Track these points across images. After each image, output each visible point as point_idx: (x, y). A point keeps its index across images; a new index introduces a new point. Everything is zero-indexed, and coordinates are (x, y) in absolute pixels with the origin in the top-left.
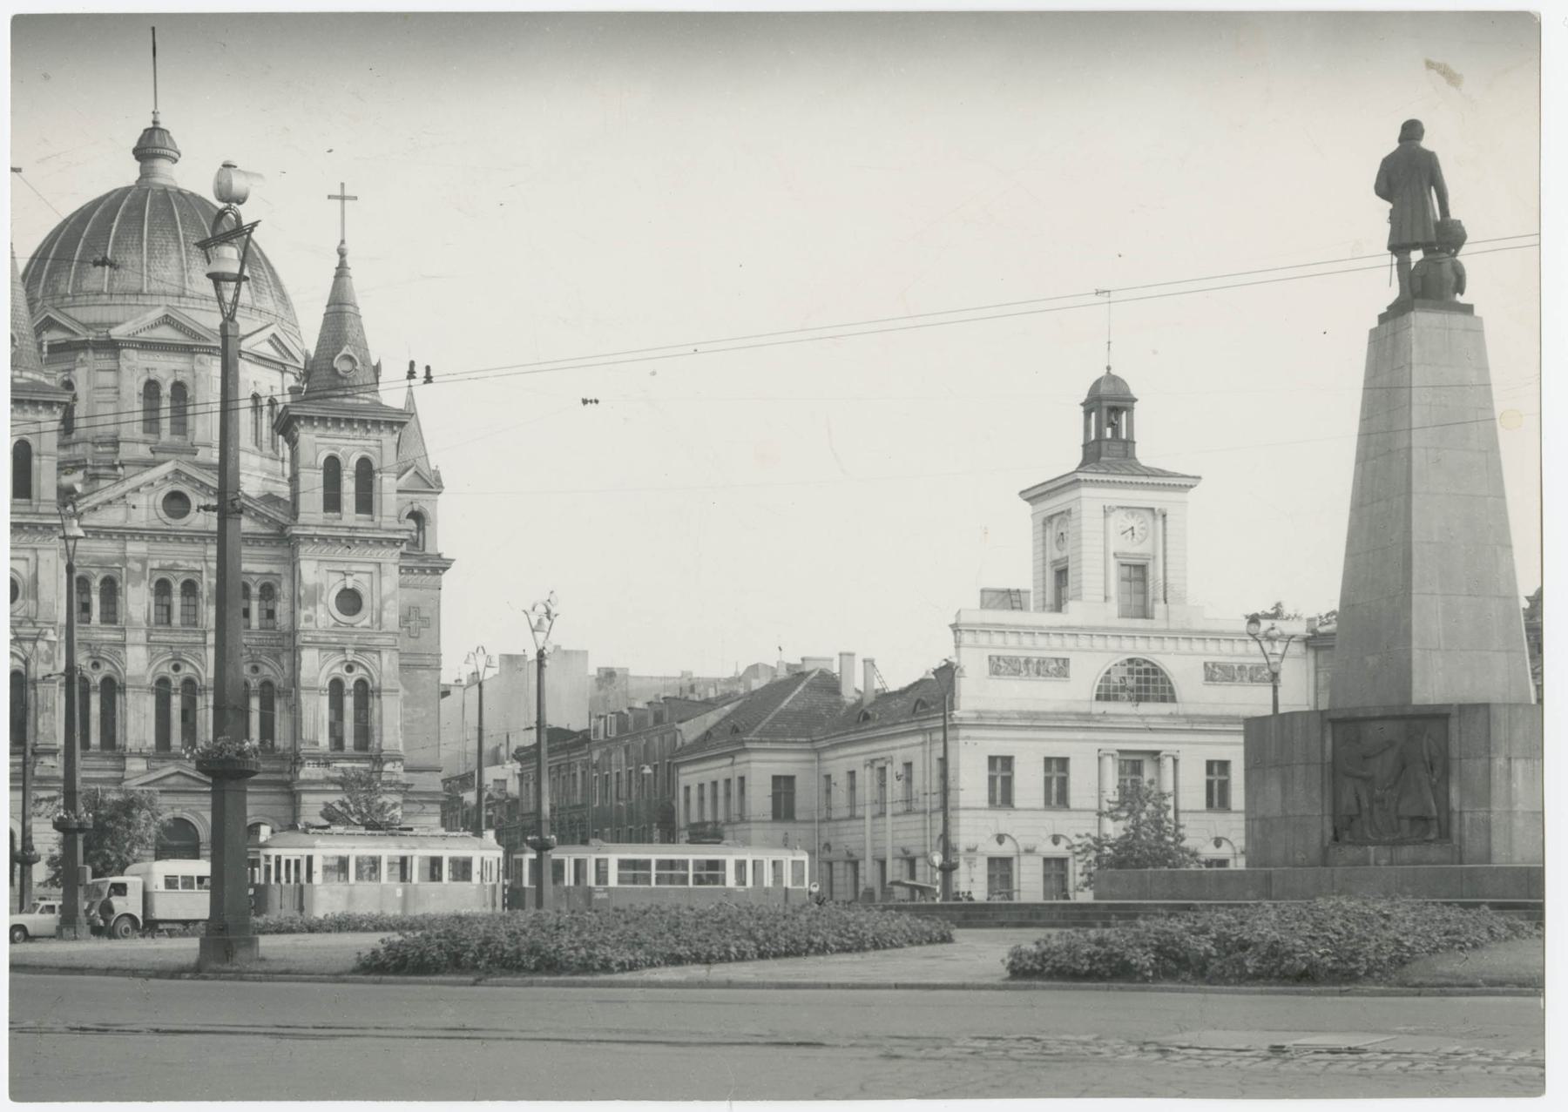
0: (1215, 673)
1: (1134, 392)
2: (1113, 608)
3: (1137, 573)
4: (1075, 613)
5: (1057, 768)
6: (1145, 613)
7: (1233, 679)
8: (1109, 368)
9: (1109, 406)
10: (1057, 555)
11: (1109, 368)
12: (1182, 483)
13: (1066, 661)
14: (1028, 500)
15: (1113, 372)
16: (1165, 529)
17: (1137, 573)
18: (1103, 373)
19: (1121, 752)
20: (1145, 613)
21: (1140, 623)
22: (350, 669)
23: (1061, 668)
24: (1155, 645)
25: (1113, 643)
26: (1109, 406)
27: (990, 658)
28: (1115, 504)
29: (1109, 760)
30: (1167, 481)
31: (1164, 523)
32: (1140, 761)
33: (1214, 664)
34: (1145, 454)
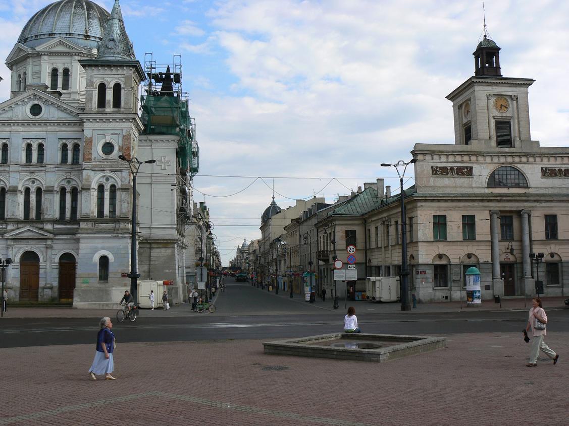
0: (547, 173)
1: (499, 45)
2: (494, 143)
3: (503, 126)
4: (474, 145)
5: (469, 222)
6: (510, 144)
7: (556, 175)
8: (485, 36)
9: (487, 54)
10: (465, 121)
11: (485, 36)
12: (527, 83)
13: (471, 168)
14: (450, 100)
15: (487, 38)
16: (517, 105)
17: (503, 126)
18: (482, 39)
19: (501, 212)
20: (510, 144)
21: (507, 150)
22: (107, 179)
23: (469, 172)
24: (517, 159)
25: (496, 159)
26: (487, 54)
27: (432, 167)
28: (492, 93)
29: (495, 216)
30: (517, 82)
31: (517, 102)
32: (511, 217)
33: (546, 169)
34: (505, 72)
